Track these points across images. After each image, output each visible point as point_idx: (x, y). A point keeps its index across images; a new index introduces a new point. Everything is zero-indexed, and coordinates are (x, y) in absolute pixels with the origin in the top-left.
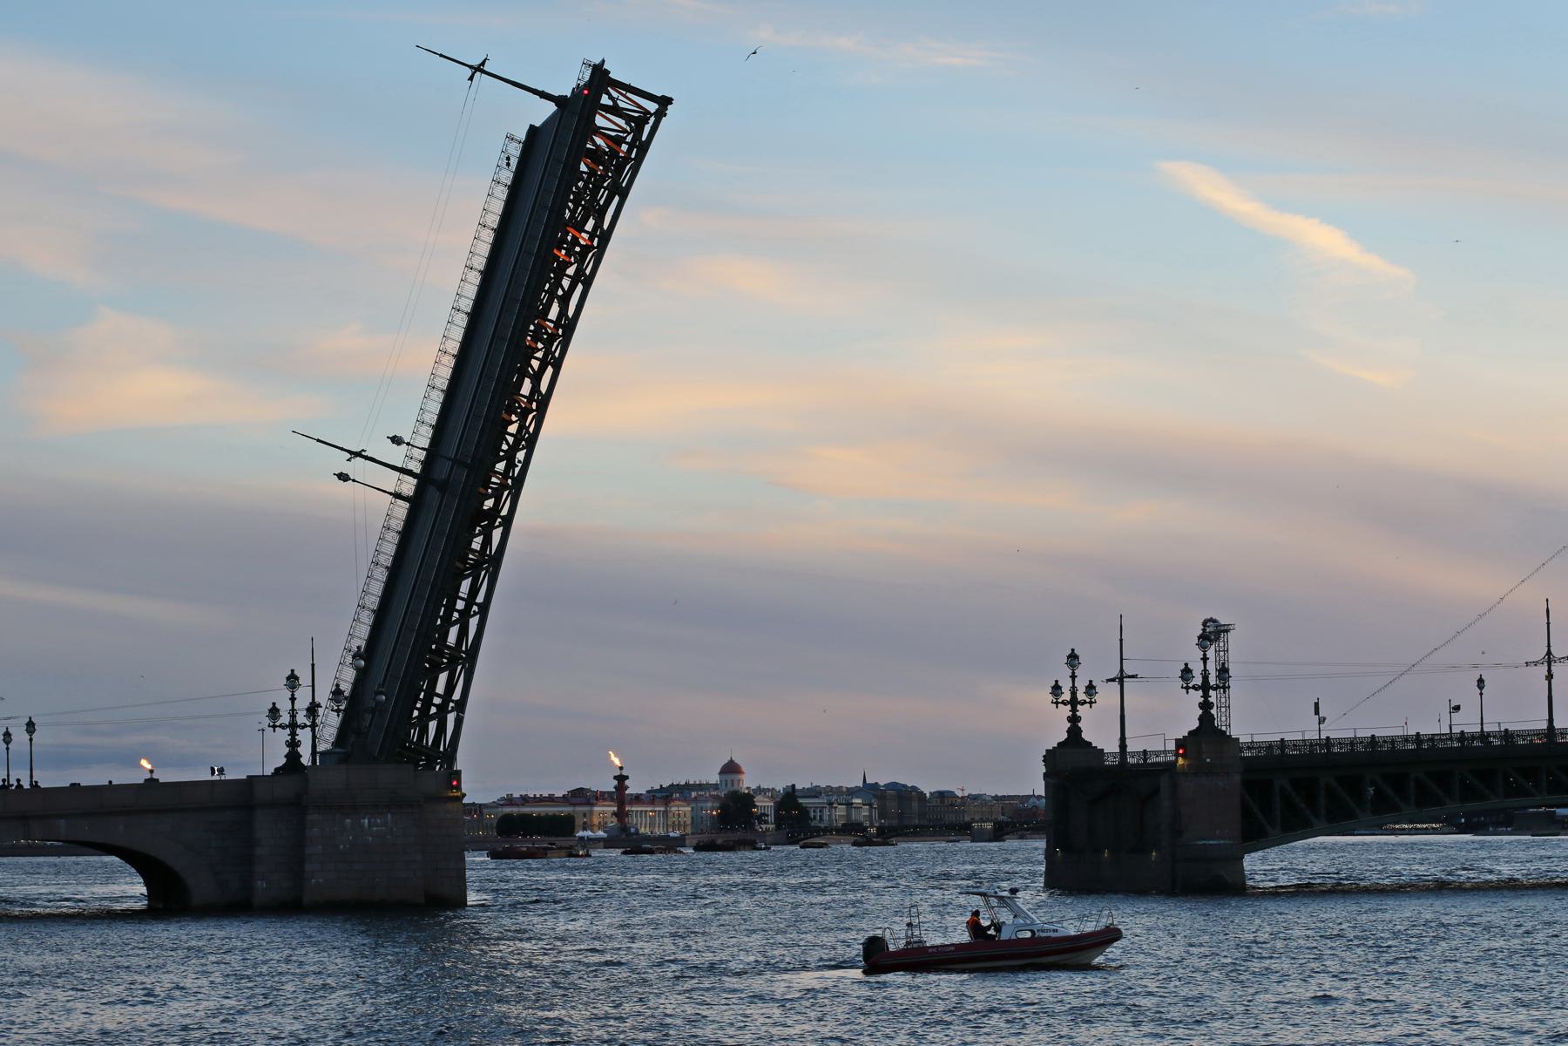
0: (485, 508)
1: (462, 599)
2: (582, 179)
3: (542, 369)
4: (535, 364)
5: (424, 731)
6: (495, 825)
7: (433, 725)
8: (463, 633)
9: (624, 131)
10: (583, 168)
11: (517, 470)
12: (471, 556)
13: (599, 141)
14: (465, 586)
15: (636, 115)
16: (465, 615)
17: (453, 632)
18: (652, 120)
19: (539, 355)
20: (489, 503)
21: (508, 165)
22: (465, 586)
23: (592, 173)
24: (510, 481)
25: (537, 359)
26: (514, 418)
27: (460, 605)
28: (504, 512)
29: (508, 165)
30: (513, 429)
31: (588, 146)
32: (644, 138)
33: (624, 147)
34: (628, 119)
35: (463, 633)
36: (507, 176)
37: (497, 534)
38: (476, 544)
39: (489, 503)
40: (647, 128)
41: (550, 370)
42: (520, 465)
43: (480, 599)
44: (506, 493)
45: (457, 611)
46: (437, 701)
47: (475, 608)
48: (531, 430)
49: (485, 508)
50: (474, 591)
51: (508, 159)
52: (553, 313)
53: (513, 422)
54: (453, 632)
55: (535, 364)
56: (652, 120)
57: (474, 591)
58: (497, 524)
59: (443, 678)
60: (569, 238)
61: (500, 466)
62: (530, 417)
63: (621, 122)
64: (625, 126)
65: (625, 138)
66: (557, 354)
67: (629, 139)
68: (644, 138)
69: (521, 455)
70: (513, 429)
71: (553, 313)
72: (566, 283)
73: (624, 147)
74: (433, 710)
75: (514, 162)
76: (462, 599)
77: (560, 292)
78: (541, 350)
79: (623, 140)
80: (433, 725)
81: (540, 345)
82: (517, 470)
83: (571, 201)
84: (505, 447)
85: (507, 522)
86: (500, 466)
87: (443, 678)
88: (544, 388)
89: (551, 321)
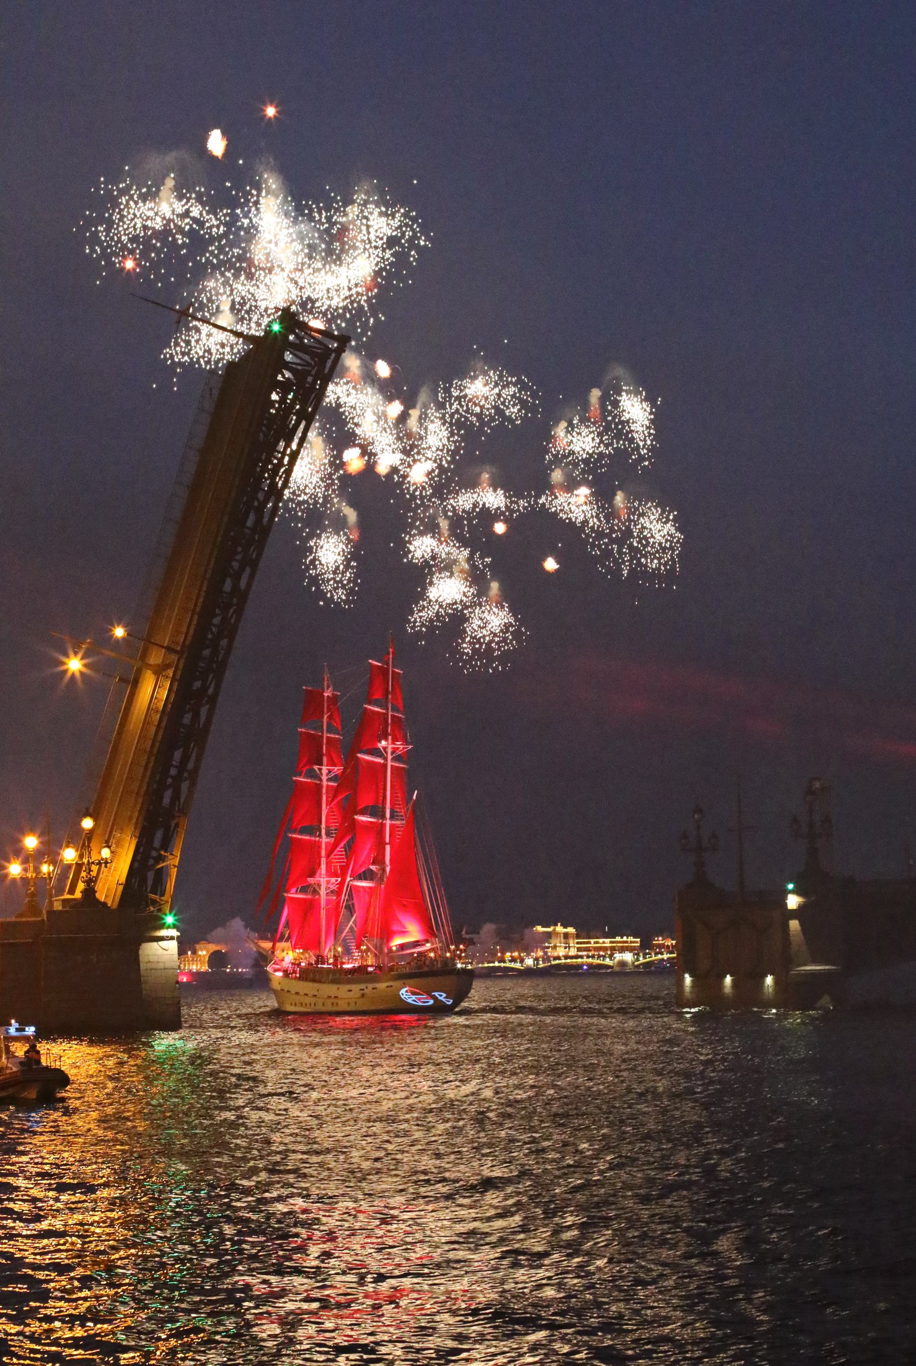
0: (194, 688)
1: (176, 767)
2: (273, 407)
3: (242, 569)
4: (235, 565)
5: (144, 880)
6: (207, 959)
7: (151, 875)
8: (176, 797)
9: (308, 364)
10: (274, 397)
11: (221, 656)
12: (181, 730)
13: (288, 374)
14: (178, 755)
15: (319, 351)
16: (178, 779)
17: (168, 794)
18: (333, 355)
19: (238, 557)
20: (197, 684)
21: (211, 395)
22: (178, 755)
23: (283, 400)
24: (214, 666)
25: (236, 560)
26: (217, 611)
27: (173, 772)
28: (211, 691)
29: (211, 395)
30: (216, 620)
31: (280, 378)
32: (327, 370)
33: (310, 379)
34: (313, 355)
35: (176, 797)
36: (209, 405)
37: (204, 711)
38: (187, 720)
39: (197, 684)
40: (329, 364)
41: (248, 570)
42: (223, 652)
43: (190, 766)
44: (211, 676)
45: (171, 777)
46: (154, 854)
47: (186, 774)
48: (233, 621)
49: (194, 688)
50: (185, 759)
51: (211, 389)
52: (250, 523)
53: (215, 615)
54: (168, 794)
55: (235, 565)
56: (333, 355)
57: (185, 759)
58: (204, 702)
59: (159, 835)
60: (263, 457)
61: (206, 652)
62: (232, 610)
63: (307, 358)
64: (310, 361)
65: (310, 371)
66: (254, 556)
67: (313, 372)
68: (327, 370)
69: (224, 642)
70: (216, 620)
71: (250, 523)
72: (261, 496)
73: (310, 379)
74: (151, 862)
75: (216, 392)
76: (176, 767)
77: (256, 504)
78: (240, 553)
79: (309, 373)
80: (151, 875)
81: (239, 549)
82: (221, 656)
83: (264, 425)
84: (210, 636)
85: (213, 700)
86: (206, 652)
87: (159, 835)
88: (243, 584)
89: (248, 528)
